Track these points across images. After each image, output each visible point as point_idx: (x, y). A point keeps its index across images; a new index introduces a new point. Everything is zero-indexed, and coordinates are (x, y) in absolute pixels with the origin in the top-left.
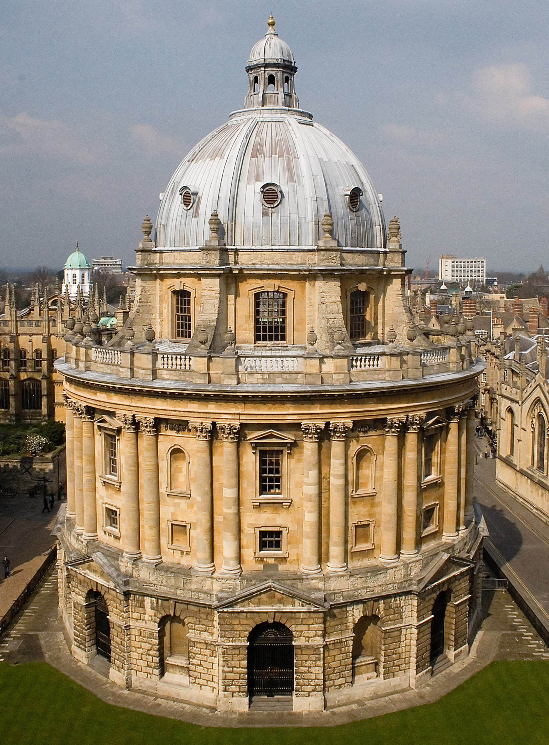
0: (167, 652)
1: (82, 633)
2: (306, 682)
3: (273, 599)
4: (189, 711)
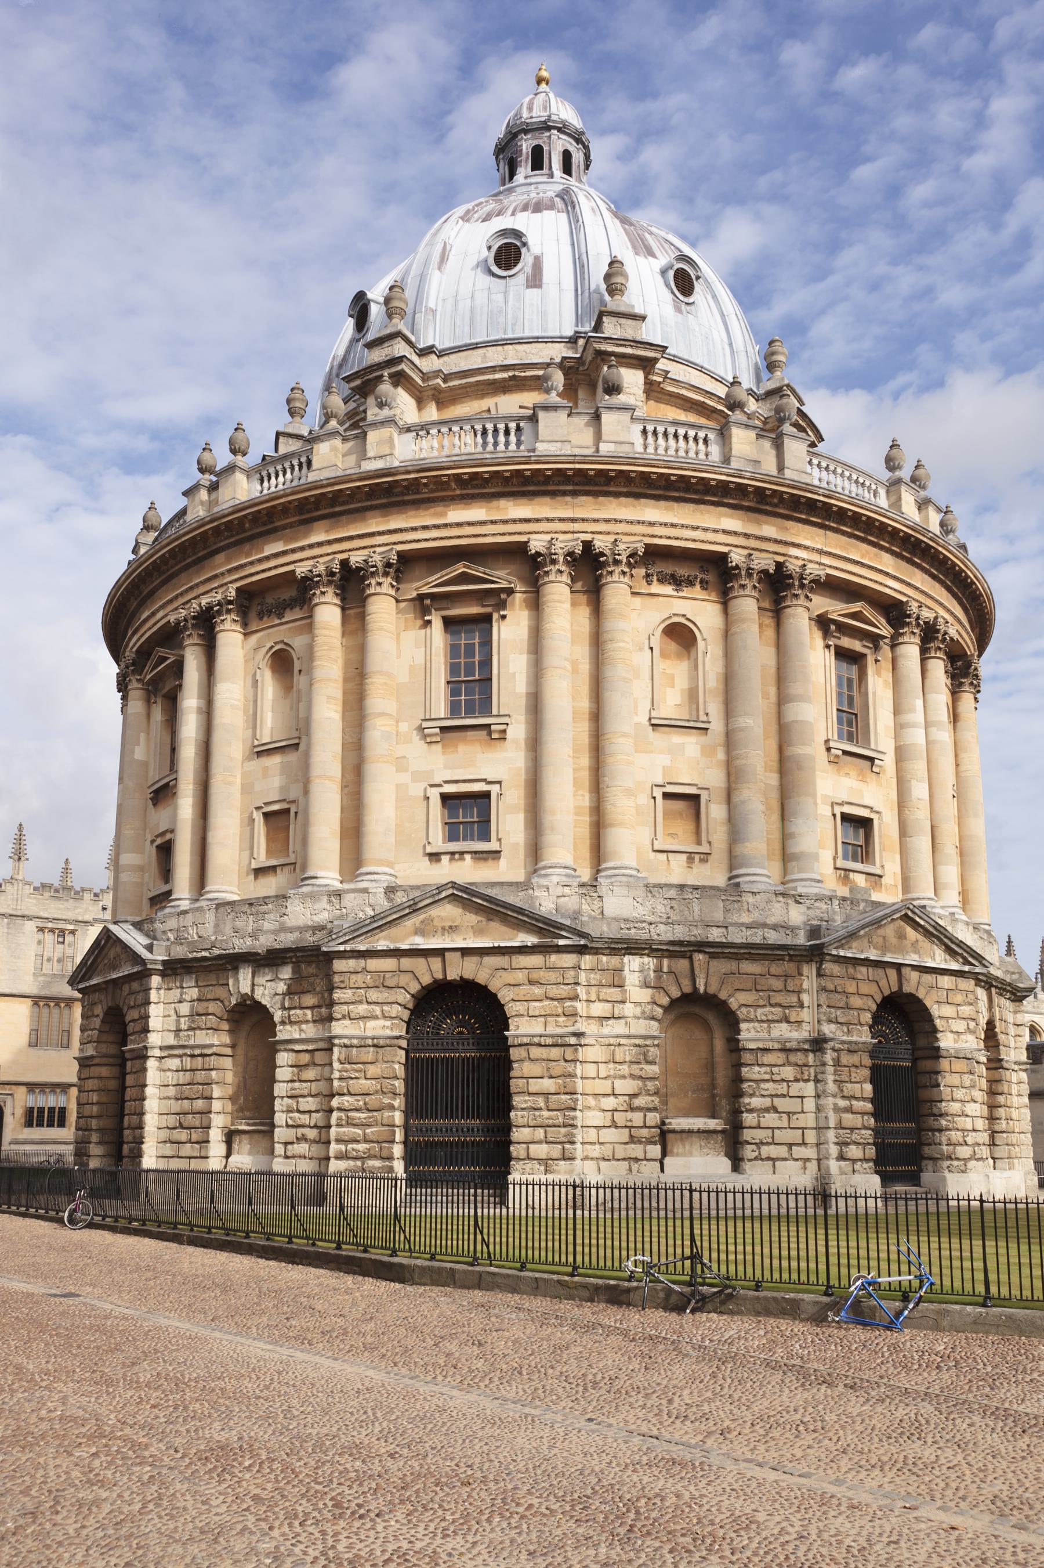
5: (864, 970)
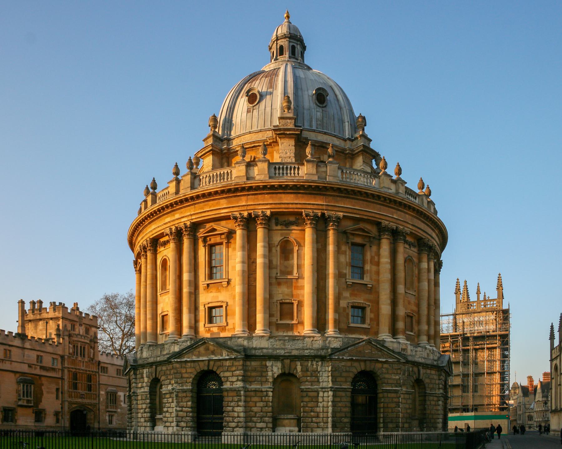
2: (231, 419)
5: (189, 364)
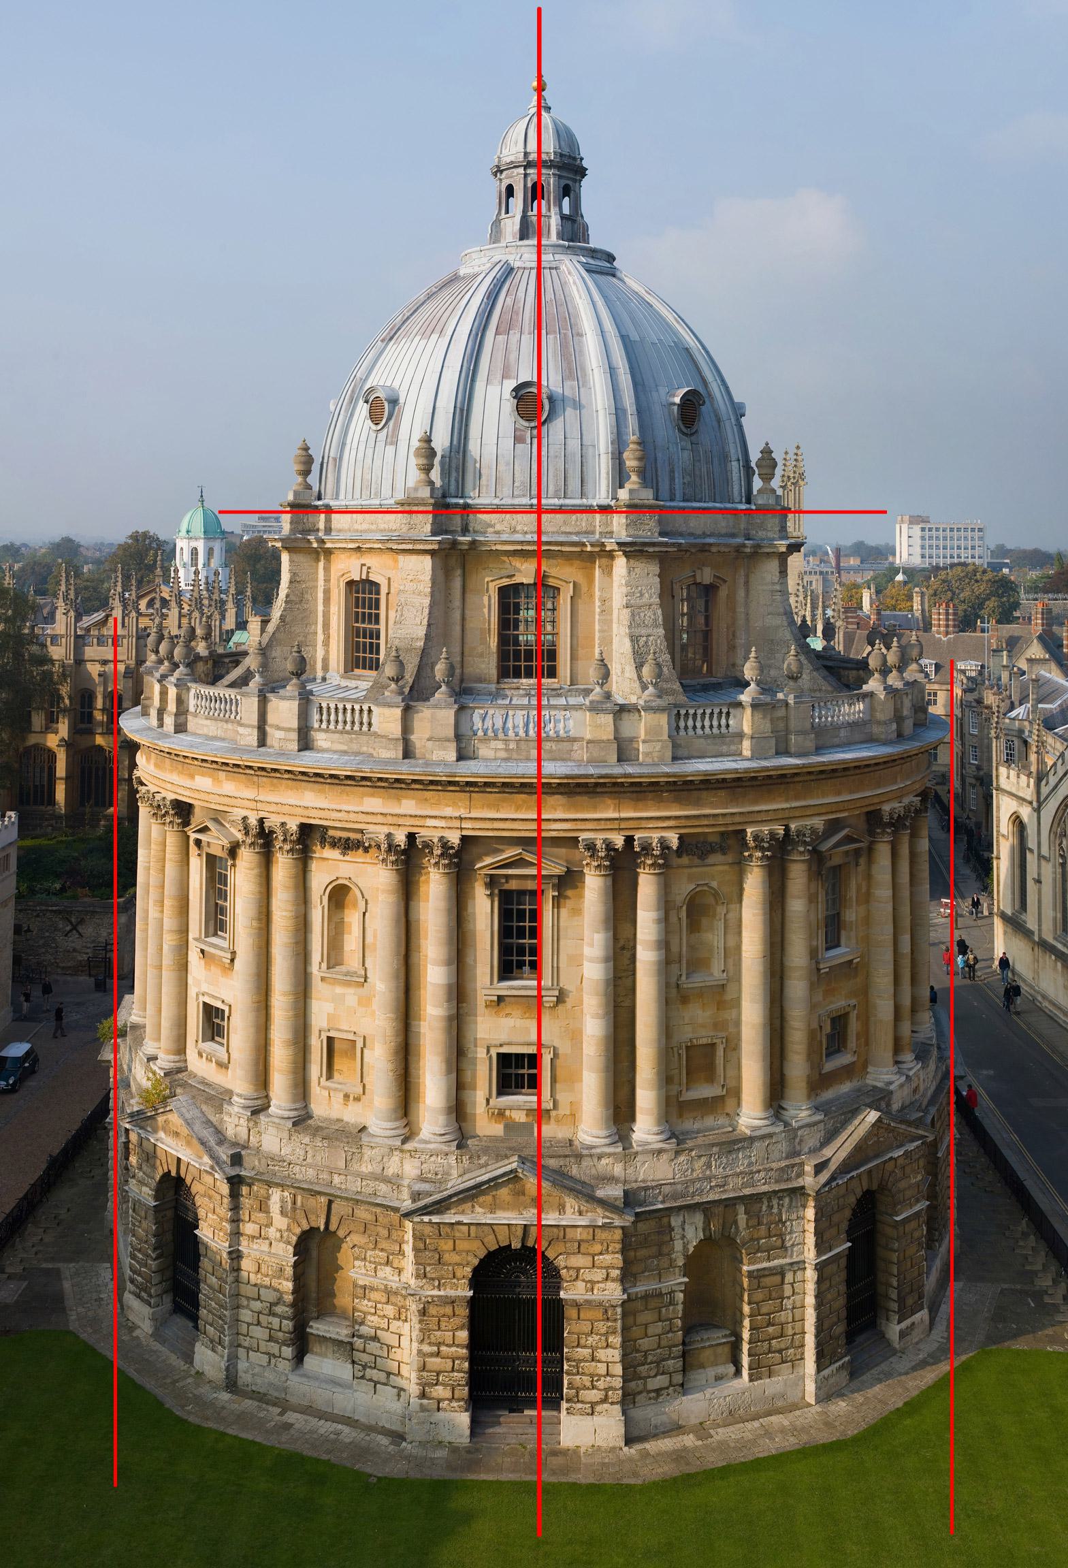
0: (313, 1310)
1: (146, 1266)
3: (522, 1198)
4: (347, 1440)
